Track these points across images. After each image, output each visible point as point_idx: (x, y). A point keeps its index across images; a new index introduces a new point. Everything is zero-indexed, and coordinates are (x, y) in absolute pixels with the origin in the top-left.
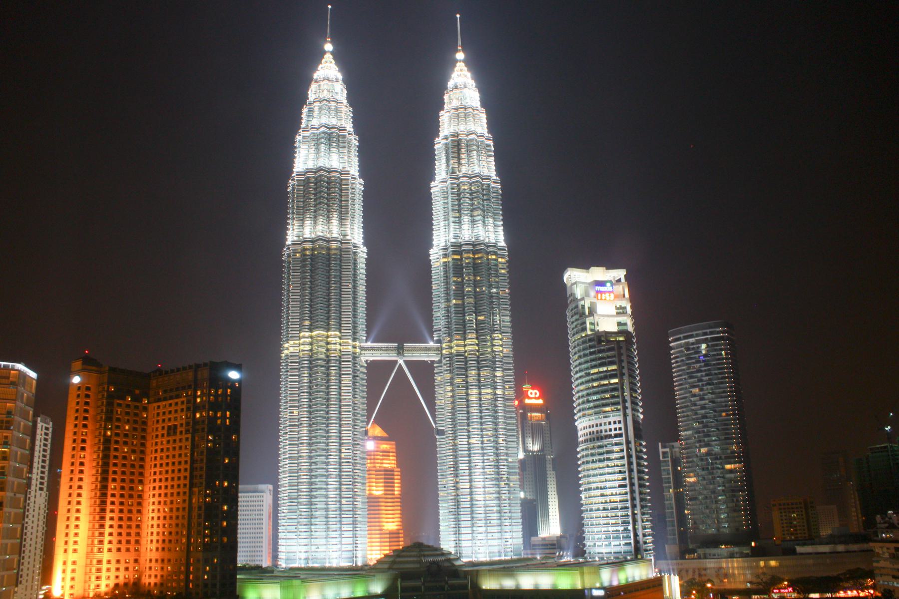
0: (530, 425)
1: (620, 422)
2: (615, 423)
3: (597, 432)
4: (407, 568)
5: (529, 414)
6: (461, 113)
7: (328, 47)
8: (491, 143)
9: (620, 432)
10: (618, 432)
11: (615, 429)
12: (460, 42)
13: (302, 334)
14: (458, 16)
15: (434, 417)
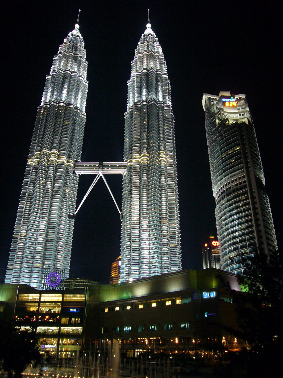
0: (214, 256)
1: (244, 177)
2: (240, 178)
3: (227, 189)
4: (74, 299)
5: (213, 250)
6: (145, 44)
7: (77, 26)
8: (163, 57)
9: (245, 184)
10: (243, 184)
11: (241, 183)
12: (149, 20)
13: (36, 153)
14: (148, 10)
15: (120, 207)
